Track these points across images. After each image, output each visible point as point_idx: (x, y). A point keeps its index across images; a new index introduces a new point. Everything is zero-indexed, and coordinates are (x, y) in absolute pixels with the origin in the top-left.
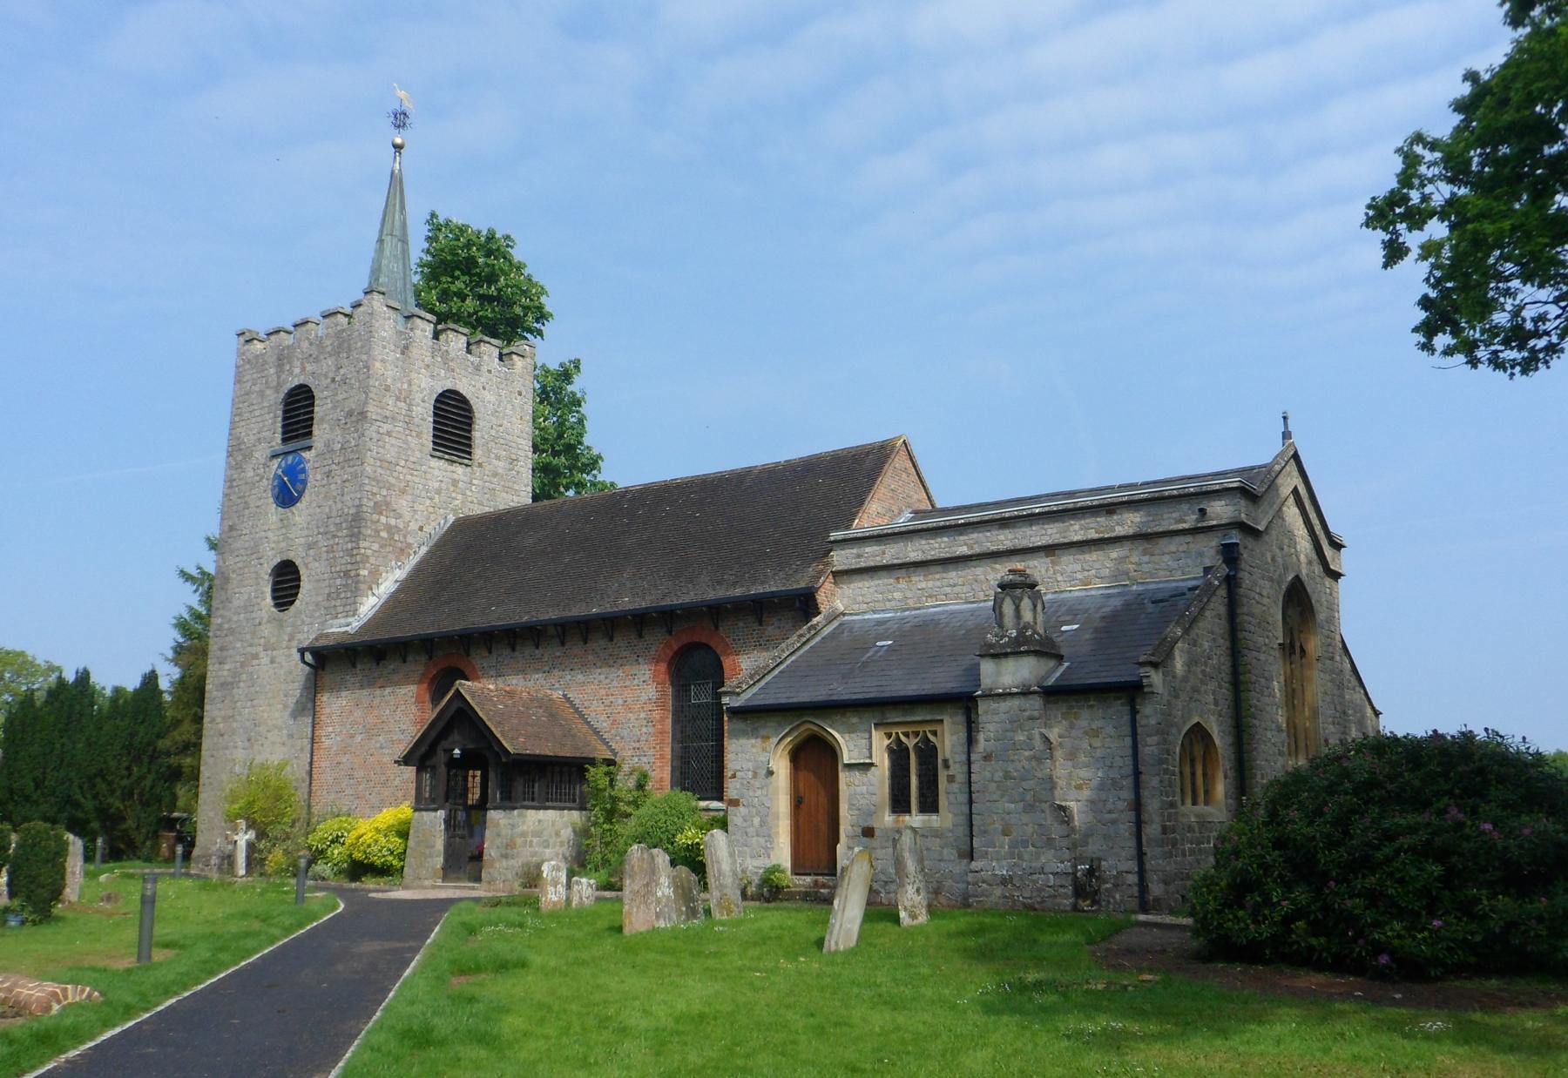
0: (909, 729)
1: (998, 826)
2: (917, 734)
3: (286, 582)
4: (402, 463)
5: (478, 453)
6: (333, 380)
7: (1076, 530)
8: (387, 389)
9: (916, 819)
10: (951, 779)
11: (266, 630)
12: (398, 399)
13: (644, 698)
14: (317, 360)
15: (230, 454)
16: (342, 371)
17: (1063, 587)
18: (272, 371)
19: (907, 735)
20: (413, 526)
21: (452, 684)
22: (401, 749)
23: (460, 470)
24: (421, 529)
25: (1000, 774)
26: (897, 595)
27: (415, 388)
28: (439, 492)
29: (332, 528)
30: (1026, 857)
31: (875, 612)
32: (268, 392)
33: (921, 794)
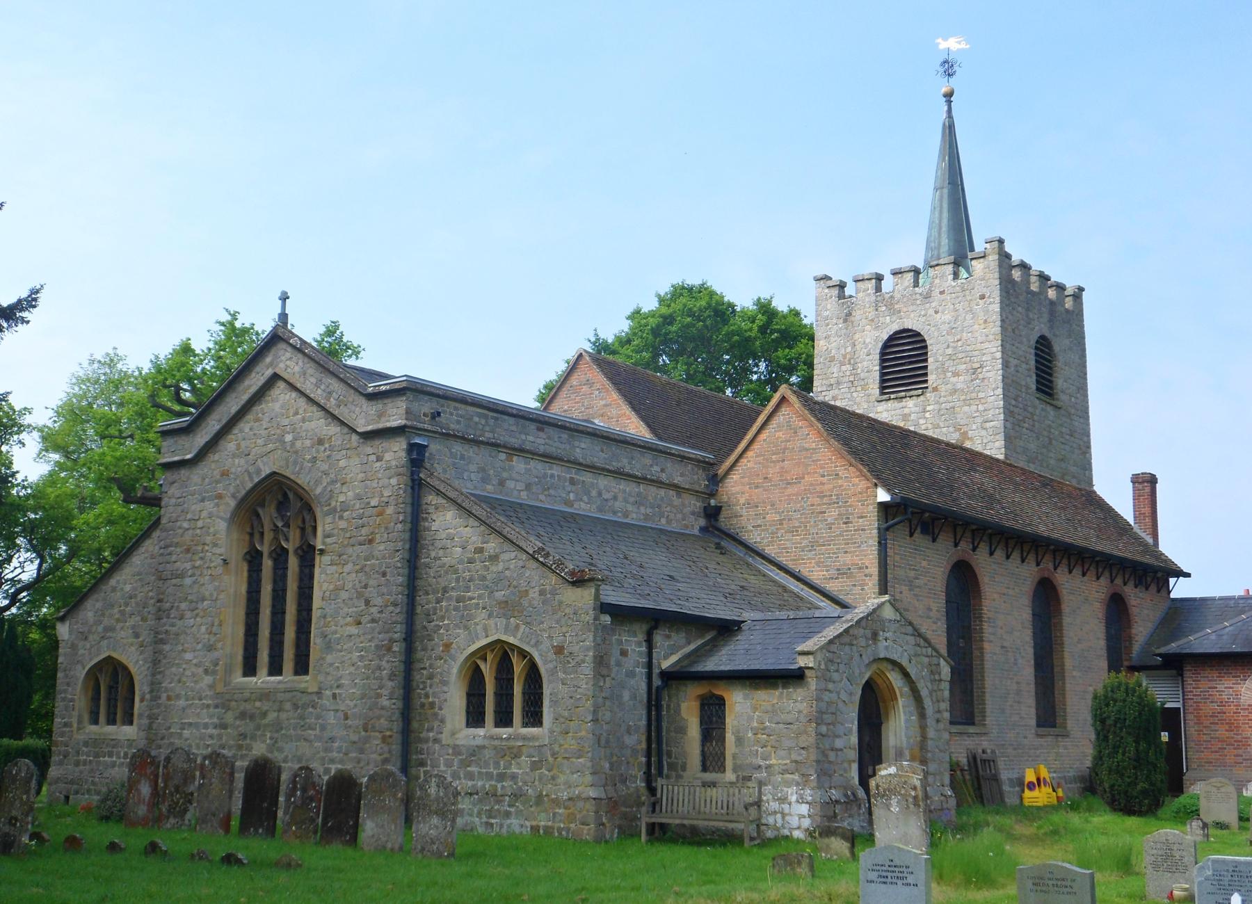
5: (931, 378)
8: (832, 359)
12: (842, 364)
27: (858, 347)
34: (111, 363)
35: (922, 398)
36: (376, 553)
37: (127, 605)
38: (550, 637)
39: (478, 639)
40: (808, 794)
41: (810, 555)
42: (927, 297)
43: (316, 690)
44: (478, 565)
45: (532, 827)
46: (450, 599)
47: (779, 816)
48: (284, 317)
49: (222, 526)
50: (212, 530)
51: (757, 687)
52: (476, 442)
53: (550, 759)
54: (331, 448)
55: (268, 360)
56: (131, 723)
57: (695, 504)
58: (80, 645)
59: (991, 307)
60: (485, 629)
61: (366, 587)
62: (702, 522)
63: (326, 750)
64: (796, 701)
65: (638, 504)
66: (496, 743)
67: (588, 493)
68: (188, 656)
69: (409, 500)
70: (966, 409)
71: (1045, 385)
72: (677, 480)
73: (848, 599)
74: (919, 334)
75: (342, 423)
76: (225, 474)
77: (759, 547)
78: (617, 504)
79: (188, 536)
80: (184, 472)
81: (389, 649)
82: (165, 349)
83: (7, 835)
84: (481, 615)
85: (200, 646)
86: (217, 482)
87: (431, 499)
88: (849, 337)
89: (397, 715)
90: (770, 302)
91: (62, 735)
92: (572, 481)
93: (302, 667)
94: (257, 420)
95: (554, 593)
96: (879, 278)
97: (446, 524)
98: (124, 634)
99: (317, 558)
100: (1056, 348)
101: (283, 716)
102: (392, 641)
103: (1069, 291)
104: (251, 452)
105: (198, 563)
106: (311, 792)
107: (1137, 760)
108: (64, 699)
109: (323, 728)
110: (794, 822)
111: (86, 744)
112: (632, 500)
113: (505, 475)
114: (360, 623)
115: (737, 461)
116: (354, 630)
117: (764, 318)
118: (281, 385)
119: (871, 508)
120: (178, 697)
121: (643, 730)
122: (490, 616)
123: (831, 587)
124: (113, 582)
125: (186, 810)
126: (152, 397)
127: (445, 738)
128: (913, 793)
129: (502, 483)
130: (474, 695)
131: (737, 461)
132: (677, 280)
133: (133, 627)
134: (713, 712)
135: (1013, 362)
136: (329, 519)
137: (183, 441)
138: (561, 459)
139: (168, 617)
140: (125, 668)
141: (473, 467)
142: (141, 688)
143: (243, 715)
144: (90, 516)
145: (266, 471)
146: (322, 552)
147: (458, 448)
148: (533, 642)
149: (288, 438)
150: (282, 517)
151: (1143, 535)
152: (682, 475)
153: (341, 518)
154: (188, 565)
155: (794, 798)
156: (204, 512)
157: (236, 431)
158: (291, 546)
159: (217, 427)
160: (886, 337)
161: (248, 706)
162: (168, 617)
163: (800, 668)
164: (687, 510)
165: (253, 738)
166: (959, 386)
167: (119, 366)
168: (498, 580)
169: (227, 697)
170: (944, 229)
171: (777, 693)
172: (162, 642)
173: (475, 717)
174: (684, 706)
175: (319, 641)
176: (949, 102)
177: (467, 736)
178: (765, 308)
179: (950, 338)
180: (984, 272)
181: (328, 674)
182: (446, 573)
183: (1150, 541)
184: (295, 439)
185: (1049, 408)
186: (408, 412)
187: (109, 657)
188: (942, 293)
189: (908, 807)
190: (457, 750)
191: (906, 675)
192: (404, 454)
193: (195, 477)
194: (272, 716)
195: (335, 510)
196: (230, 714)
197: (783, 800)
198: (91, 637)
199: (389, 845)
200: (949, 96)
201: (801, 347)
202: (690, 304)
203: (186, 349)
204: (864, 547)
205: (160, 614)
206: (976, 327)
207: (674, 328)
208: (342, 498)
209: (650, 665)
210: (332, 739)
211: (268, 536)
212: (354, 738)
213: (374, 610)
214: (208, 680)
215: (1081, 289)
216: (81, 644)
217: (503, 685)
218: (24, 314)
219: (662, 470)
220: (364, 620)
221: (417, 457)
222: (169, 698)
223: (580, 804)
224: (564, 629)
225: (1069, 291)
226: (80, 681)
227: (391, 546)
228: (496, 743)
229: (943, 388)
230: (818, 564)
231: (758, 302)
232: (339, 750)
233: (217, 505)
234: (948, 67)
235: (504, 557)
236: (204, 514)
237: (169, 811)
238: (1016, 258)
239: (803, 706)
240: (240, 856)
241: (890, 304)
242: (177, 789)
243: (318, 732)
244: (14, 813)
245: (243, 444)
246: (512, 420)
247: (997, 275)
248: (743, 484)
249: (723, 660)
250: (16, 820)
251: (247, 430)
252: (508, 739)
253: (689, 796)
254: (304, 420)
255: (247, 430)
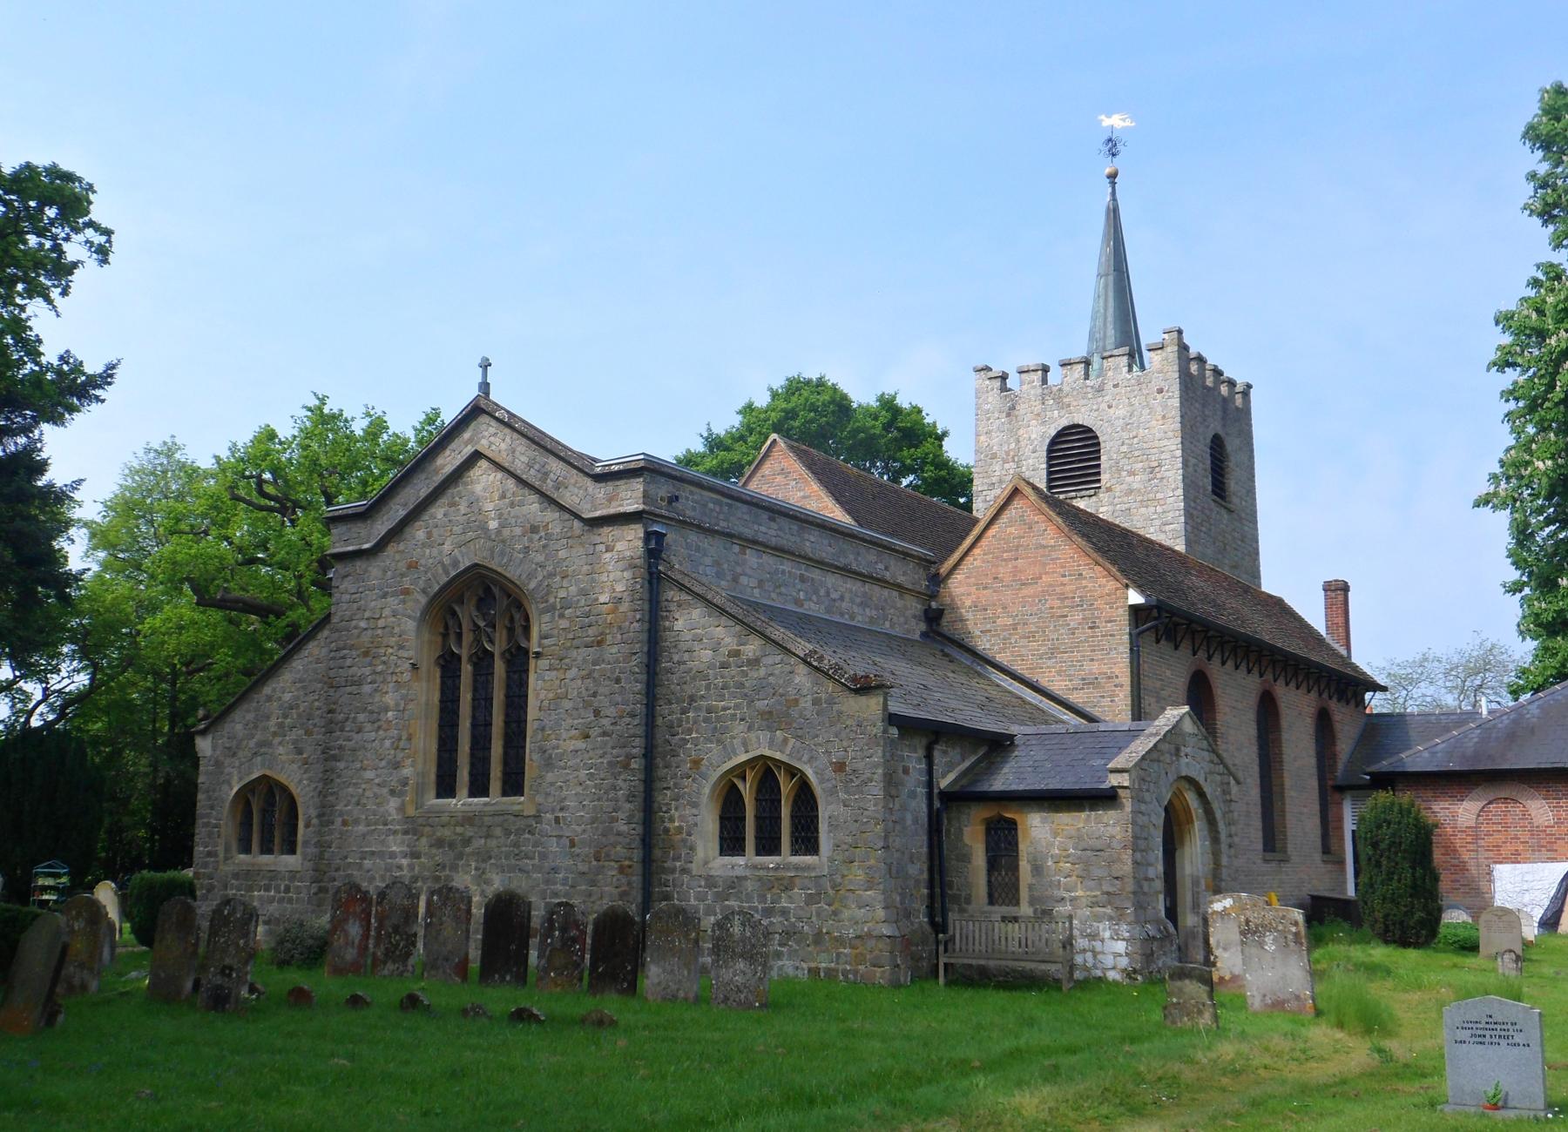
5: (1104, 477)
8: (994, 456)
12: (1005, 461)
34: (169, 451)
36: (607, 657)
37: (285, 716)
38: (828, 752)
39: (736, 755)
40: (1124, 930)
41: (1050, 663)
42: (1100, 390)
43: (533, 813)
44: (734, 671)
45: (810, 970)
46: (699, 709)
47: (1089, 954)
48: (485, 387)
49: (410, 625)
50: (397, 630)
51: (1058, 810)
52: (711, 532)
53: (831, 892)
54: (548, 537)
55: (466, 435)
56: (293, 852)
57: (915, 606)
58: (226, 763)
59: (1170, 402)
60: (745, 744)
61: (595, 695)
62: (923, 627)
63: (547, 882)
64: (1107, 825)
65: (863, 605)
66: (762, 873)
67: (816, 592)
68: (369, 774)
69: (646, 596)
70: (1143, 510)
71: (1219, 489)
72: (901, 579)
73: (1096, 712)
74: (1090, 430)
75: (562, 508)
76: (413, 566)
77: (989, 654)
78: (844, 605)
79: (366, 637)
80: (359, 565)
81: (626, 766)
82: (244, 437)
83: (221, 987)
84: (739, 728)
85: (383, 763)
86: (403, 575)
87: (672, 594)
88: (1013, 432)
89: (637, 843)
90: (894, 398)
91: (205, 865)
92: (803, 579)
93: (514, 785)
94: (453, 504)
95: (831, 702)
96: (1045, 369)
97: (688, 623)
98: (282, 751)
99: (532, 662)
100: (1229, 448)
101: (493, 843)
102: (630, 757)
103: (1239, 388)
104: (442, 545)
105: (379, 668)
106: (574, 933)
107: (1414, 886)
108: (206, 825)
109: (543, 856)
110: (1109, 961)
111: (236, 876)
112: (858, 600)
113: (739, 570)
114: (587, 736)
115: (962, 559)
116: (581, 744)
117: (889, 415)
118: (483, 464)
119: (1121, 611)
120: (357, 822)
121: (924, 858)
122: (750, 729)
123: (1076, 698)
124: (267, 690)
125: (408, 955)
126: (232, 488)
127: (695, 868)
128: (1294, 929)
129: (735, 580)
130: (729, 819)
131: (962, 559)
132: (793, 373)
133: (295, 742)
134: (1002, 839)
135: (1193, 461)
136: (546, 617)
137: (359, 529)
138: (793, 554)
139: (342, 730)
140: (284, 789)
141: (708, 561)
142: (307, 810)
143: (439, 843)
144: (156, 621)
145: (465, 563)
146: (538, 655)
147: (693, 537)
148: (805, 758)
149: (493, 525)
150: (484, 616)
151: (1336, 646)
152: (905, 574)
153: (562, 616)
154: (367, 671)
155: (1107, 934)
156: (387, 613)
157: (426, 517)
158: (497, 647)
159: (402, 513)
160: (1053, 433)
161: (446, 833)
162: (342, 730)
163: (1113, 787)
164: (909, 613)
165: (454, 868)
166: (1135, 486)
167: (177, 456)
168: (761, 686)
169: (420, 821)
170: (1110, 319)
171: (1083, 815)
172: (335, 758)
173: (731, 843)
174: (967, 831)
175: (535, 757)
176: (1113, 184)
177: (724, 866)
178: (888, 404)
179: (1125, 435)
180: (1161, 365)
181: (548, 794)
182: (693, 678)
183: (1344, 652)
184: (502, 526)
185: (1223, 511)
186: (646, 495)
187: (264, 776)
188: (1116, 386)
189: (1287, 945)
190: (711, 882)
191: (1201, 794)
192: (640, 544)
193: (374, 571)
194: (479, 843)
195: (552, 608)
196: (424, 840)
197: (1094, 936)
198: (240, 754)
199: (681, 994)
200: (1113, 177)
201: (928, 446)
202: (813, 398)
203: (271, 435)
204: (1113, 654)
205: (332, 725)
206: (1154, 423)
207: (797, 424)
208: (562, 594)
209: (930, 784)
210: (555, 870)
211: (468, 638)
212: (582, 867)
213: (605, 722)
214: (393, 803)
215: (1249, 386)
216: (227, 762)
217: (771, 809)
218: (98, 392)
219: (886, 568)
220: (594, 732)
221: (655, 549)
222: (345, 823)
223: (873, 942)
224: (845, 744)
225: (1239, 388)
226: (227, 804)
227: (626, 648)
228: (762, 873)
229: (1117, 488)
230: (1059, 673)
231: (881, 399)
232: (565, 882)
233: (404, 602)
234: (1112, 146)
235: (769, 660)
236: (386, 612)
237: (386, 955)
238: (1193, 352)
239: (1117, 832)
240: (535, 1011)
241: (1059, 397)
242: (396, 929)
243: (536, 861)
244: (228, 961)
245: (435, 532)
246: (745, 508)
247: (1176, 368)
248: (969, 585)
249: (1005, 779)
250: (231, 969)
251: (440, 516)
252: (776, 869)
253: (983, 930)
254: (512, 505)
255: (440, 516)
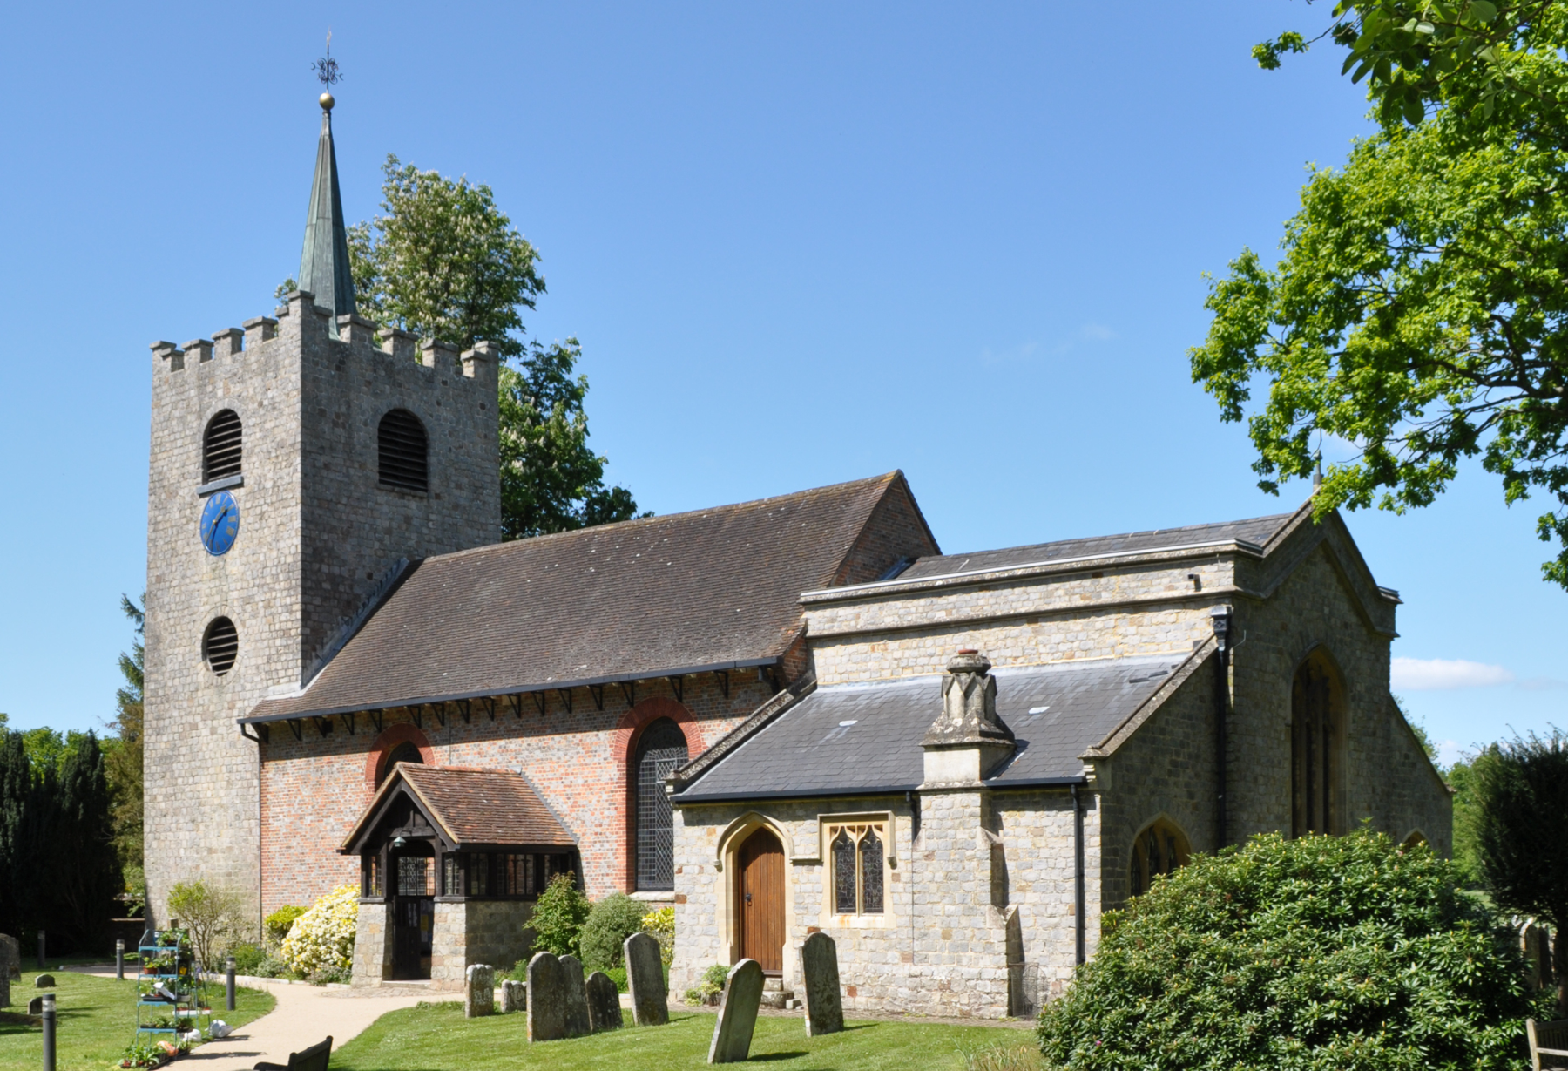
0: (856, 824)
1: (938, 930)
2: (861, 829)
3: (220, 642)
4: (344, 500)
5: (435, 482)
6: (261, 404)
7: (1061, 595)
9: (859, 920)
10: (896, 878)
11: (204, 696)
12: (335, 424)
13: (605, 778)
14: (242, 381)
15: (152, 492)
16: (270, 394)
17: (1046, 659)
18: (192, 393)
19: (852, 829)
20: (360, 574)
21: (390, 767)
22: (342, 836)
23: (413, 504)
24: (370, 576)
25: (940, 875)
26: (872, 665)
28: (389, 531)
29: (269, 580)
30: (965, 961)
31: (848, 683)
32: (191, 418)
33: (867, 894)
35: (425, 502)
160: (385, 411)
166: (462, 502)
188: (445, 383)
